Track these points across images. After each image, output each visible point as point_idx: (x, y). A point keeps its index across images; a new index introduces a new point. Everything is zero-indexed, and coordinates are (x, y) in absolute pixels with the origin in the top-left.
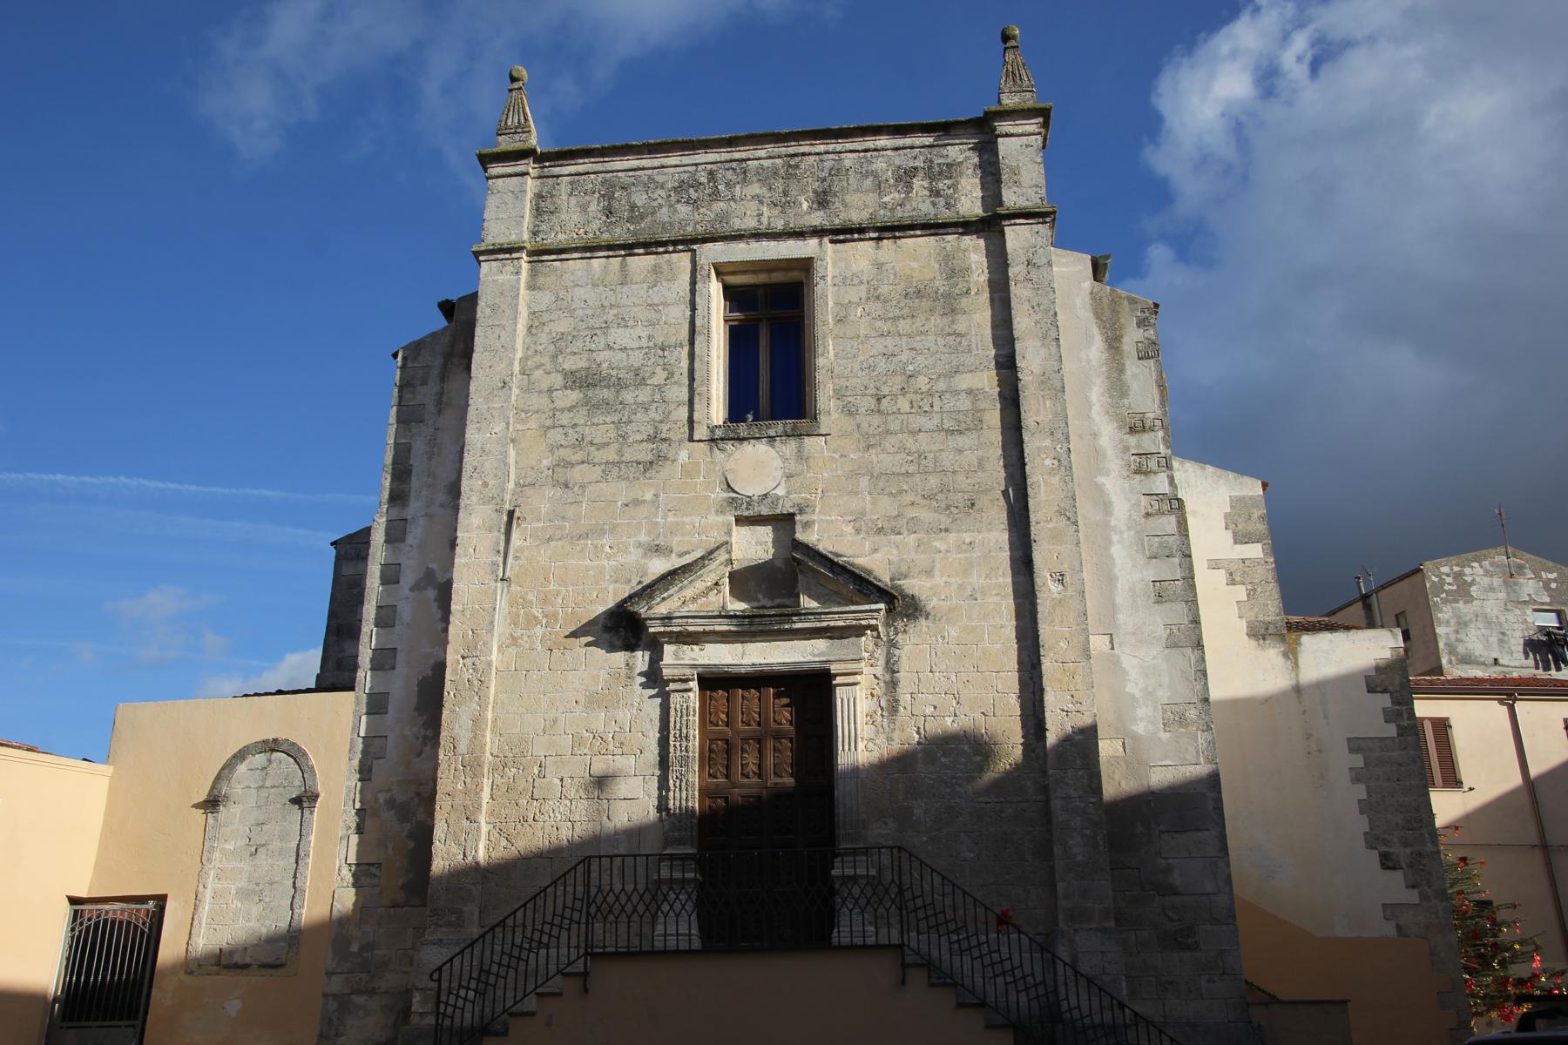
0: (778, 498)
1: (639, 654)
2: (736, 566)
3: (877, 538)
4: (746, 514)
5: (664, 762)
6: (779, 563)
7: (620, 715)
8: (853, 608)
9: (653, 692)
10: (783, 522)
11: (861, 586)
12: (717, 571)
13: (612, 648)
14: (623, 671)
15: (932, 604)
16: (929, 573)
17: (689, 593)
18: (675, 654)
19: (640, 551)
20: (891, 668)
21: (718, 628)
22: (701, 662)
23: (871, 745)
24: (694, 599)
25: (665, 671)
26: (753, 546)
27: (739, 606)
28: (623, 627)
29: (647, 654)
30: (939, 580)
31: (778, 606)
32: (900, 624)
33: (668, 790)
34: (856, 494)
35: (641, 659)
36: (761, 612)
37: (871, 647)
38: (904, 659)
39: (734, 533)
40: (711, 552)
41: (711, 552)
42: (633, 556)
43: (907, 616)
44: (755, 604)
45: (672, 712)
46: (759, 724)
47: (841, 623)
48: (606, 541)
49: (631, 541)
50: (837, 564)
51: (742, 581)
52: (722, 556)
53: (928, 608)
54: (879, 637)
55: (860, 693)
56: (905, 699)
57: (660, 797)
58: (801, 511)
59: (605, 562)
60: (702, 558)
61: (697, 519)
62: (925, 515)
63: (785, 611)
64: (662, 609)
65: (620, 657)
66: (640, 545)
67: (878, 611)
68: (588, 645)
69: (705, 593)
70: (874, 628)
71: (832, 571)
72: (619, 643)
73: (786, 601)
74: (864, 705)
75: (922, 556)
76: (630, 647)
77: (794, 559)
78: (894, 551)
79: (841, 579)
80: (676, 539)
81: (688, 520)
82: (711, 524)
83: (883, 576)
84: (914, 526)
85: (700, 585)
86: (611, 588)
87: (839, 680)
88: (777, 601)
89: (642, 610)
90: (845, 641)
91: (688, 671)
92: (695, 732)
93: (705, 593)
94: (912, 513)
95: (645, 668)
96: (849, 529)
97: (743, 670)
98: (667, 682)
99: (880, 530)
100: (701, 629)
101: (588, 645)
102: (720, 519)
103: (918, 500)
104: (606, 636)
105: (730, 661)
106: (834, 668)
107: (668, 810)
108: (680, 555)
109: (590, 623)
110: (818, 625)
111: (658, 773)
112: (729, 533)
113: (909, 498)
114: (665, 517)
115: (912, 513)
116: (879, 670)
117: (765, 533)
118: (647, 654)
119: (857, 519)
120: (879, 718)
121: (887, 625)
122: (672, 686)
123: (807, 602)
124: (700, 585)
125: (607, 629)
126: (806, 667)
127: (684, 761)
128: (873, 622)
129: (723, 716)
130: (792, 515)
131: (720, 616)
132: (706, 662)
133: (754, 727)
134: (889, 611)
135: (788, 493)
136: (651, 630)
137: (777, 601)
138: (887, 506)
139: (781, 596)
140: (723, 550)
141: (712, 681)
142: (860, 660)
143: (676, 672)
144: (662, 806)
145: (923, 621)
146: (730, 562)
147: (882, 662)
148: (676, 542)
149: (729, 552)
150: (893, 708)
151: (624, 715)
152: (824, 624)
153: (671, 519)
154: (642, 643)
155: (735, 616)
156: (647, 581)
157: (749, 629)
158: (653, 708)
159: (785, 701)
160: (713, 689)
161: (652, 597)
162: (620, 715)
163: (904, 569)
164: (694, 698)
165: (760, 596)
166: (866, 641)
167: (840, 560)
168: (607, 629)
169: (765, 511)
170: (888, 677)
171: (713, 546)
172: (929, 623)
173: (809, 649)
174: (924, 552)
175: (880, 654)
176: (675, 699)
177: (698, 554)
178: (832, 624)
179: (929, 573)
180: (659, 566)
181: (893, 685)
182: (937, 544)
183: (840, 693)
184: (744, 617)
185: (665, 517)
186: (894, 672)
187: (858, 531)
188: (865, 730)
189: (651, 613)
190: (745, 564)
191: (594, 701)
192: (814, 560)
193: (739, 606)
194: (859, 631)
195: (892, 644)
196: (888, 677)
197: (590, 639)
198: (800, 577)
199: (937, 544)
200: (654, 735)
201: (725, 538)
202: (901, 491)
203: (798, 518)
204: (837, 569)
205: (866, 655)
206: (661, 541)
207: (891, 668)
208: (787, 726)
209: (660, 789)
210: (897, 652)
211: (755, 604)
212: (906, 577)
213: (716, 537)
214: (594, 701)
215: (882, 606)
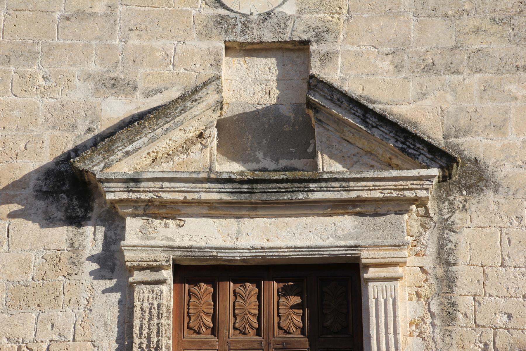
0: (287, 18)
1: (89, 230)
2: (227, 113)
3: (425, 78)
4: (241, 39)
6: (286, 111)
7: (59, 317)
8: (395, 173)
10: (294, 51)
11: (410, 144)
12: (200, 117)
13: (49, 221)
14: (65, 255)
15: (504, 171)
16: (499, 128)
17: (162, 146)
18: (143, 231)
19: (90, 85)
20: (446, 258)
21: (204, 196)
22: (178, 242)
24: (169, 156)
25: (129, 255)
26: (252, 85)
27: (231, 168)
28: (68, 191)
29: (101, 231)
30: (513, 138)
31: (285, 169)
32: (457, 198)
34: (397, 15)
35: (92, 238)
36: (266, 175)
37: (416, 228)
38: (463, 246)
39: (224, 67)
40: (196, 90)
41: (196, 90)
42: (80, 93)
43: (469, 187)
44: (254, 166)
45: (137, 313)
46: (258, 332)
47: (377, 194)
48: (37, 69)
49: (77, 71)
50: (373, 113)
51: (235, 132)
52: (210, 97)
53: (499, 177)
54: (427, 215)
56: (465, 303)
58: (319, 38)
59: (37, 99)
60: (183, 98)
61: (170, 44)
62: (497, 47)
63: (299, 175)
64: (124, 168)
65: (61, 234)
66: (88, 77)
67: (429, 178)
68: (12, 215)
69: (185, 148)
70: (420, 202)
71: (364, 122)
72: (59, 215)
73: (296, 163)
74: (407, 310)
75: (490, 105)
76: (75, 220)
77: (310, 104)
78: (450, 97)
79: (376, 132)
80: (142, 71)
81: (158, 44)
82: (196, 53)
83: (436, 135)
84: (477, 61)
85: (178, 137)
86: (47, 136)
87: (372, 273)
88: (284, 163)
89: (94, 166)
90: (380, 220)
91: (161, 256)
93: (185, 148)
94: (476, 43)
95: (98, 250)
96: (386, 65)
97: (237, 256)
98: (130, 271)
99: (430, 68)
100: (180, 197)
101: (12, 215)
102: (204, 45)
103: (486, 24)
104: (41, 204)
105: (218, 242)
106: (366, 256)
108: (148, 94)
109: (18, 185)
110: (345, 195)
112: (217, 65)
113: (472, 22)
114: (124, 40)
115: (476, 43)
116: (428, 262)
117: (267, 68)
118: (101, 231)
119: (397, 51)
120: (429, 329)
121: (440, 199)
122: (137, 276)
123: (328, 165)
124: (178, 137)
125: (42, 194)
126: (326, 253)
128: (422, 194)
129: (208, 321)
130: (306, 43)
131: (209, 180)
132: (186, 242)
133: (251, 334)
134: (444, 179)
135: (301, 11)
136: (110, 197)
137: (284, 163)
138: (440, 33)
139: (290, 156)
140: (212, 87)
141: (194, 272)
142: (401, 246)
143: (144, 255)
145: (490, 195)
146: (220, 105)
147: (432, 250)
148: (142, 75)
149: (219, 91)
150: (449, 313)
151: (65, 318)
152: (353, 195)
153: (134, 41)
154: (93, 215)
155: (229, 181)
156: (101, 128)
157: (250, 197)
158: (109, 307)
159: (295, 300)
160: (194, 281)
161: (110, 151)
162: (59, 317)
163: (463, 122)
164: (167, 290)
165: (260, 155)
166: (410, 220)
167: (378, 108)
168: (42, 194)
169: (268, 36)
170: (440, 272)
171: (193, 84)
172: (500, 198)
173: (331, 229)
174: (492, 99)
175: (430, 239)
177: (174, 94)
178: (364, 195)
179: (499, 128)
180: (116, 109)
181: (448, 282)
182: (512, 88)
183: (374, 292)
184: (242, 182)
185: (124, 40)
186: (449, 264)
187: (398, 68)
189: (109, 173)
190: (239, 110)
191: (21, 297)
192: (338, 103)
193: (231, 168)
194: (400, 206)
195: (447, 226)
197: (15, 207)
198: (318, 130)
199: (512, 88)
201: (211, 73)
202: (461, 13)
203: (314, 47)
204: (372, 120)
205: (410, 239)
206: (120, 73)
207: (446, 258)
208: (297, 335)
210: (453, 237)
211: (254, 166)
212: (465, 133)
213: (198, 71)
214: (21, 297)
215: (435, 171)
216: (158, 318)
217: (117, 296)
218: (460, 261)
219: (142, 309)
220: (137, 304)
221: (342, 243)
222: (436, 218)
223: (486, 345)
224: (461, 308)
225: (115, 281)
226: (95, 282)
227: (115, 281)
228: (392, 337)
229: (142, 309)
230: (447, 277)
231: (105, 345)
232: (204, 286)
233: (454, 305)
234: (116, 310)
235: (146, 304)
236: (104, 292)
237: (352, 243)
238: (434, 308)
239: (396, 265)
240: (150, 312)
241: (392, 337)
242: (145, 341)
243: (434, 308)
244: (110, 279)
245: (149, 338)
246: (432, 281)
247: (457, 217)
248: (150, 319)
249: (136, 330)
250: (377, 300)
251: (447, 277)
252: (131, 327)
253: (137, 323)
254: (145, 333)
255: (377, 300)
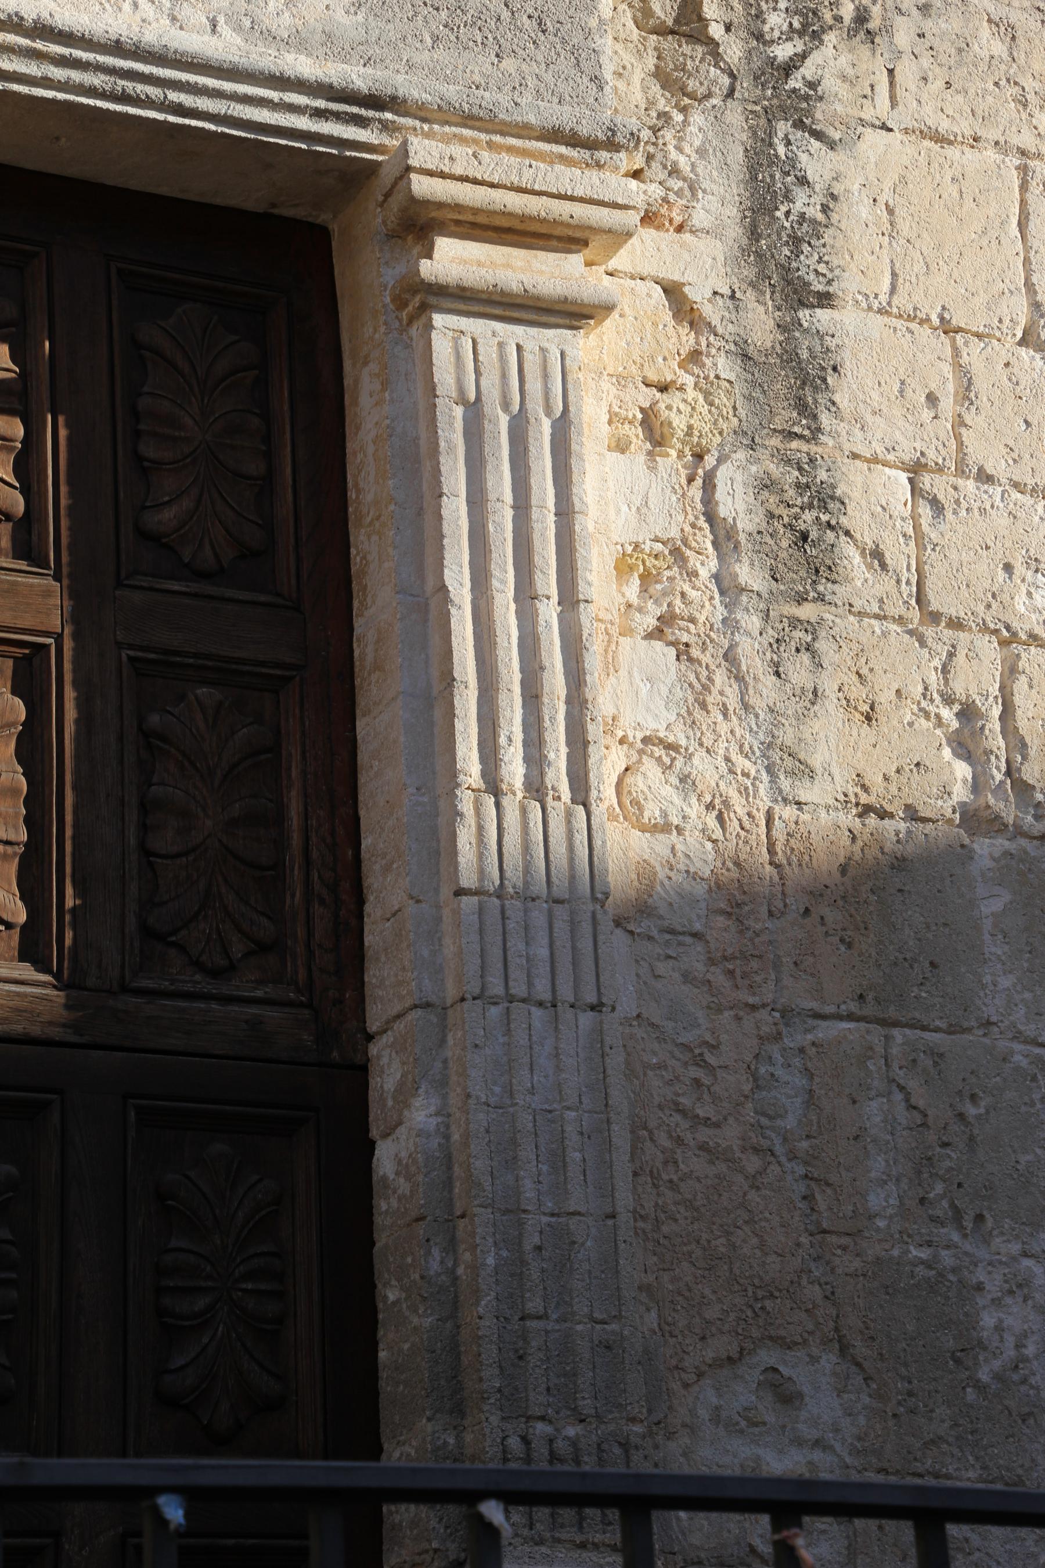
20: (784, 258)
23: (655, 787)
38: (858, 214)
55: (602, 370)
56: (875, 499)
87: (451, 259)
106: (439, 163)
116: (706, 263)
120: (710, 609)
126: (211, 106)
150: (806, 538)
175: (709, 145)
181: (796, 382)
188: (634, 690)
196: (760, 322)
218: (849, 285)
221: (303, 66)
222: (733, 50)
223: (968, 713)
224: (856, 518)
228: (549, 612)
230: (789, 357)
233: (824, 498)
237: (358, 77)
238: (735, 501)
239: (565, 238)
241: (549, 612)
243: (735, 501)
246: (725, 366)
247: (830, 62)
250: (474, 411)
251: (789, 357)
255: (474, 411)
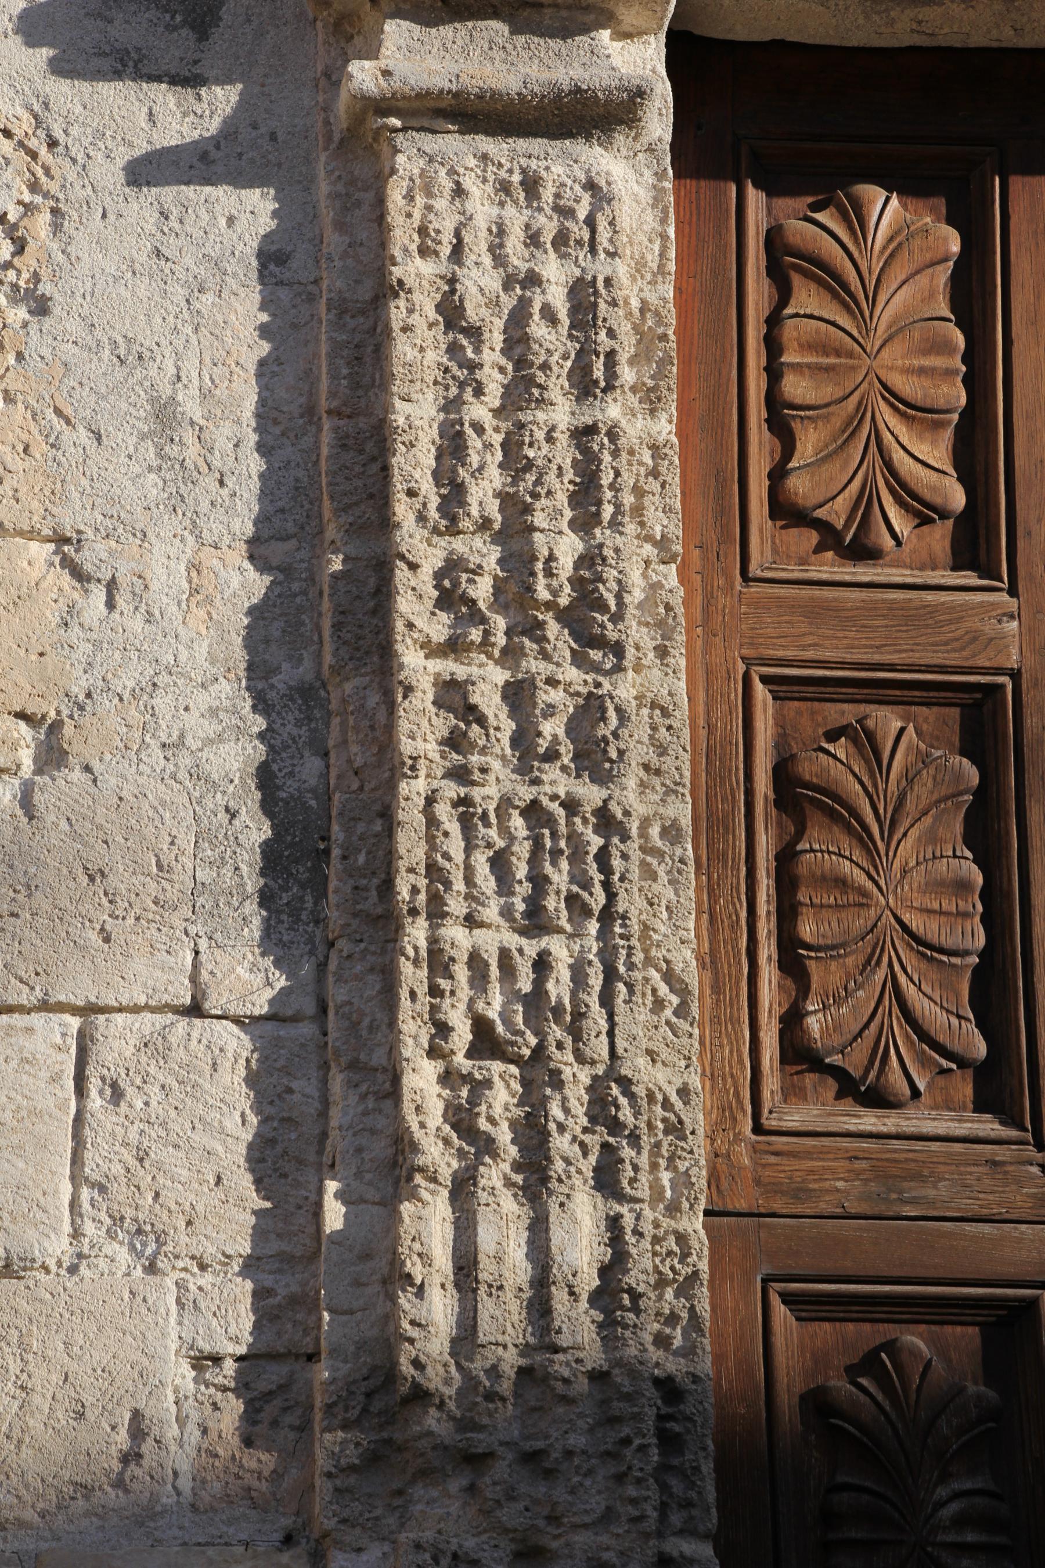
5: (324, 864)
9: (179, 117)
33: (392, 1171)
45: (417, 346)
57: (283, 1258)
92: (645, 571)
107: (383, 1392)
111: (250, 980)
127: (568, 866)
129: (927, 459)
144: (319, 1364)
160: (823, 175)
176: (448, 197)
200: (198, 585)
209: (281, 1160)
216: (584, 387)
217: (249, 213)
219: (451, 312)
220: (417, 272)
225: (222, 99)
226: (66, 94)
227: (222, 99)
229: (451, 312)
231: (165, 569)
232: (885, 210)
234: (241, 317)
235: (480, 281)
236: (143, 172)
240: (517, 340)
242: (487, 555)
244: (188, 79)
245: (514, 528)
248: (523, 390)
249: (415, 464)
252: (371, 445)
253: (416, 415)
254: (484, 493)
